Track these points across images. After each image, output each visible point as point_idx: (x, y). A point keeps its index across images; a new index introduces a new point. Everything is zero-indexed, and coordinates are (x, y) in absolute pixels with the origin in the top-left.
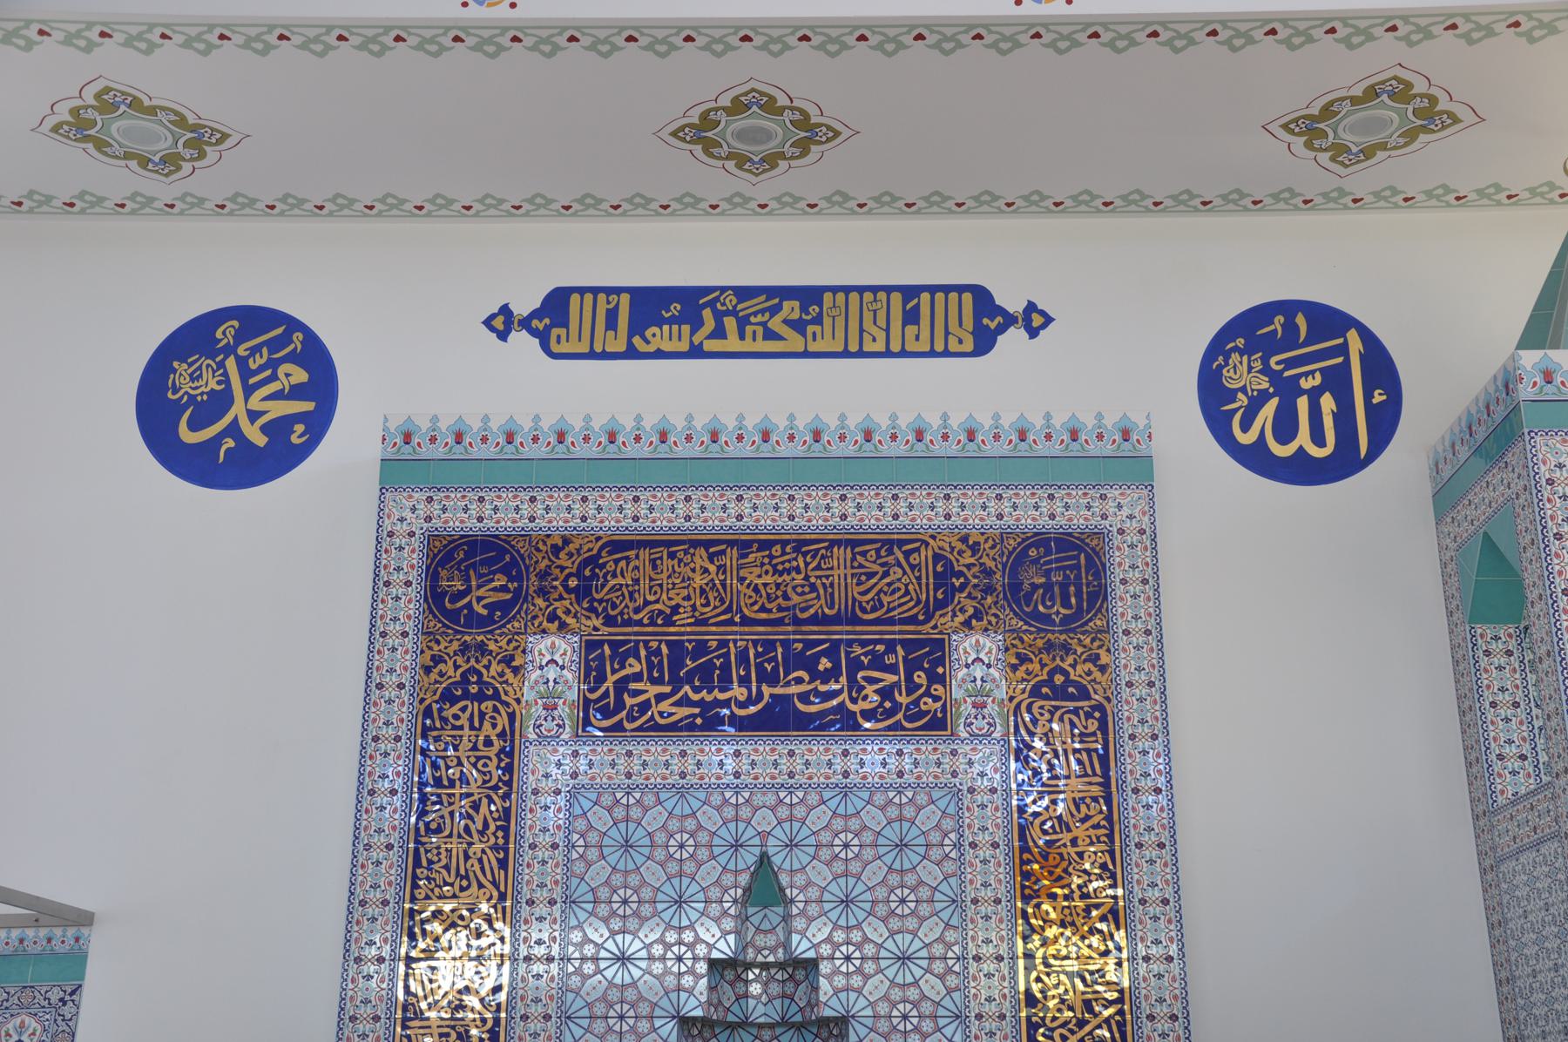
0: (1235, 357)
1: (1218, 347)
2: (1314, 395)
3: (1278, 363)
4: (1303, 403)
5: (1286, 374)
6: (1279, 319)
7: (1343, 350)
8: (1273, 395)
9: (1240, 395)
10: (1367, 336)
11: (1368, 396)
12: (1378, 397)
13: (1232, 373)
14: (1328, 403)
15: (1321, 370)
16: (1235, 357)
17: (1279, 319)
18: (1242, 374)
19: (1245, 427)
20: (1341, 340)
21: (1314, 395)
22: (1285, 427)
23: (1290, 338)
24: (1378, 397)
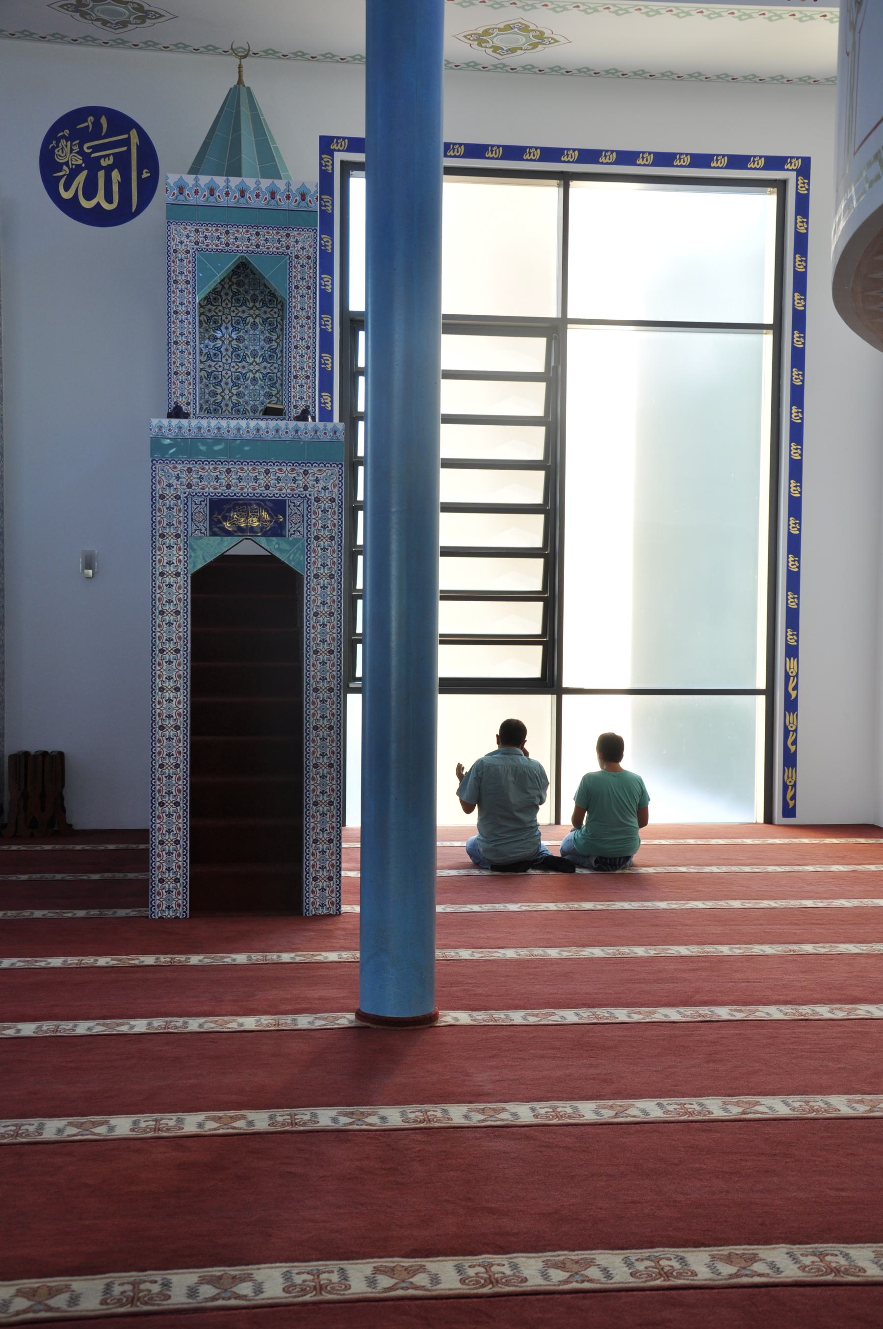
0: (63, 142)
1: (53, 135)
2: (109, 170)
3: (88, 148)
4: (101, 174)
5: (93, 155)
6: (91, 119)
7: (127, 142)
8: (82, 169)
9: (65, 167)
10: (142, 134)
11: (139, 173)
12: (145, 175)
13: (60, 153)
14: (116, 175)
15: (113, 154)
16: (63, 142)
17: (91, 119)
18: (67, 154)
19: (67, 188)
20: (126, 136)
21: (109, 170)
22: (90, 191)
23: (96, 133)
24: (145, 175)
